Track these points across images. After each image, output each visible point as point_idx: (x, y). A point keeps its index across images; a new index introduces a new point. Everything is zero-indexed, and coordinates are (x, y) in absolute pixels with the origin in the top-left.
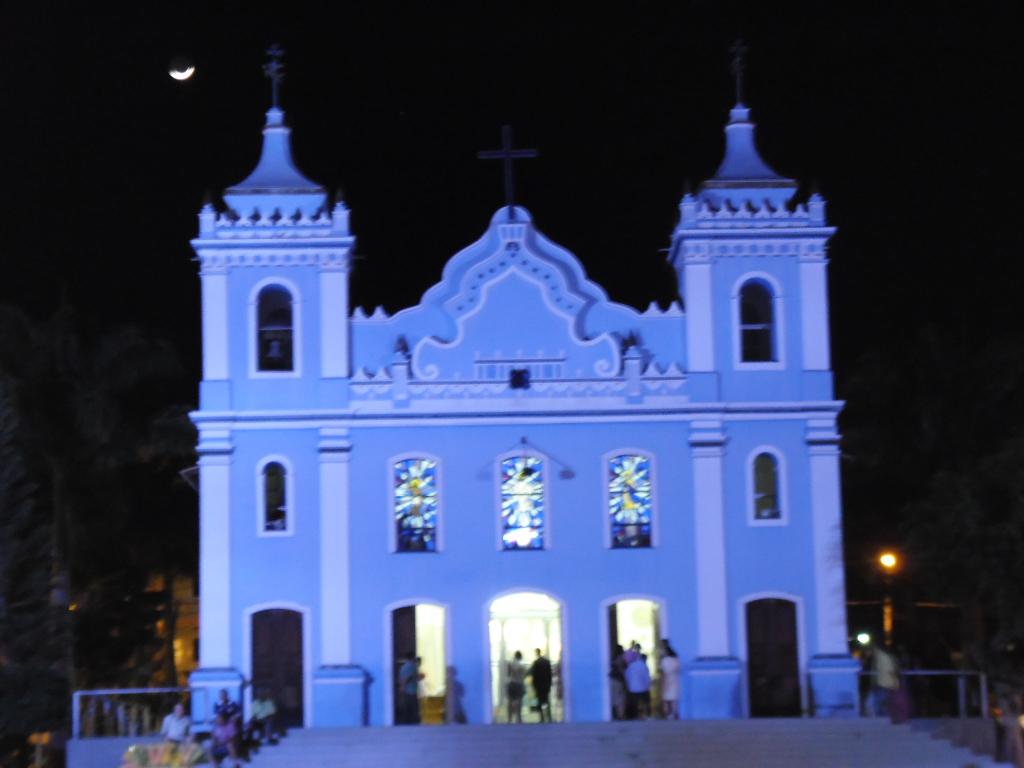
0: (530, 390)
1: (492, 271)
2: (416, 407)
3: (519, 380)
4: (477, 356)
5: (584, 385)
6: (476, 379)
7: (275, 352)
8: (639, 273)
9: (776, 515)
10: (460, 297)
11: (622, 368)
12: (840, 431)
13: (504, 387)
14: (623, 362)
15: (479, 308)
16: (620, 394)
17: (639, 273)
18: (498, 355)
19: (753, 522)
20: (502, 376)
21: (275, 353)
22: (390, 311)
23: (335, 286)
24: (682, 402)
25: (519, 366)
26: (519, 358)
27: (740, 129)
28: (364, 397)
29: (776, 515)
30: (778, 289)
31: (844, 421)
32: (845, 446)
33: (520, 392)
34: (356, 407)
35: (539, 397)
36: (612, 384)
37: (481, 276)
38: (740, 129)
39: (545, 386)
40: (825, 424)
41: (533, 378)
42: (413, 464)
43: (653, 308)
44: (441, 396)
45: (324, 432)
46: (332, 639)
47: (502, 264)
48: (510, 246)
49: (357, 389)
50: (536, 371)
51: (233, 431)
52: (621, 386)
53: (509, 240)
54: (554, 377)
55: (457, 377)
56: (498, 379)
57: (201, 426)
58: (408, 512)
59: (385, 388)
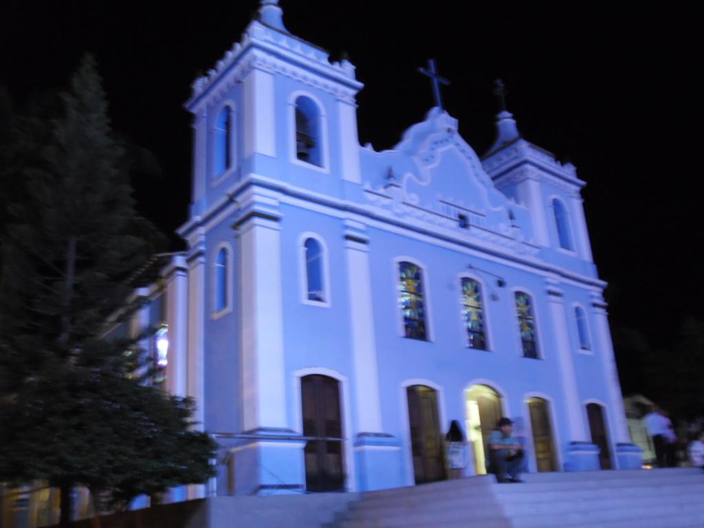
1: (442, 142)
2: (407, 221)
3: (463, 222)
4: (440, 196)
10: (424, 150)
12: (605, 301)
13: (454, 224)
16: (512, 248)
21: (307, 147)
22: (378, 148)
23: (347, 117)
25: (463, 213)
27: (507, 122)
28: (371, 203)
31: (606, 294)
32: (608, 309)
33: (464, 231)
35: (472, 236)
38: (507, 122)
40: (596, 293)
42: (409, 269)
45: (349, 223)
46: (369, 409)
50: (472, 218)
51: (280, 203)
55: (429, 207)
58: (409, 305)
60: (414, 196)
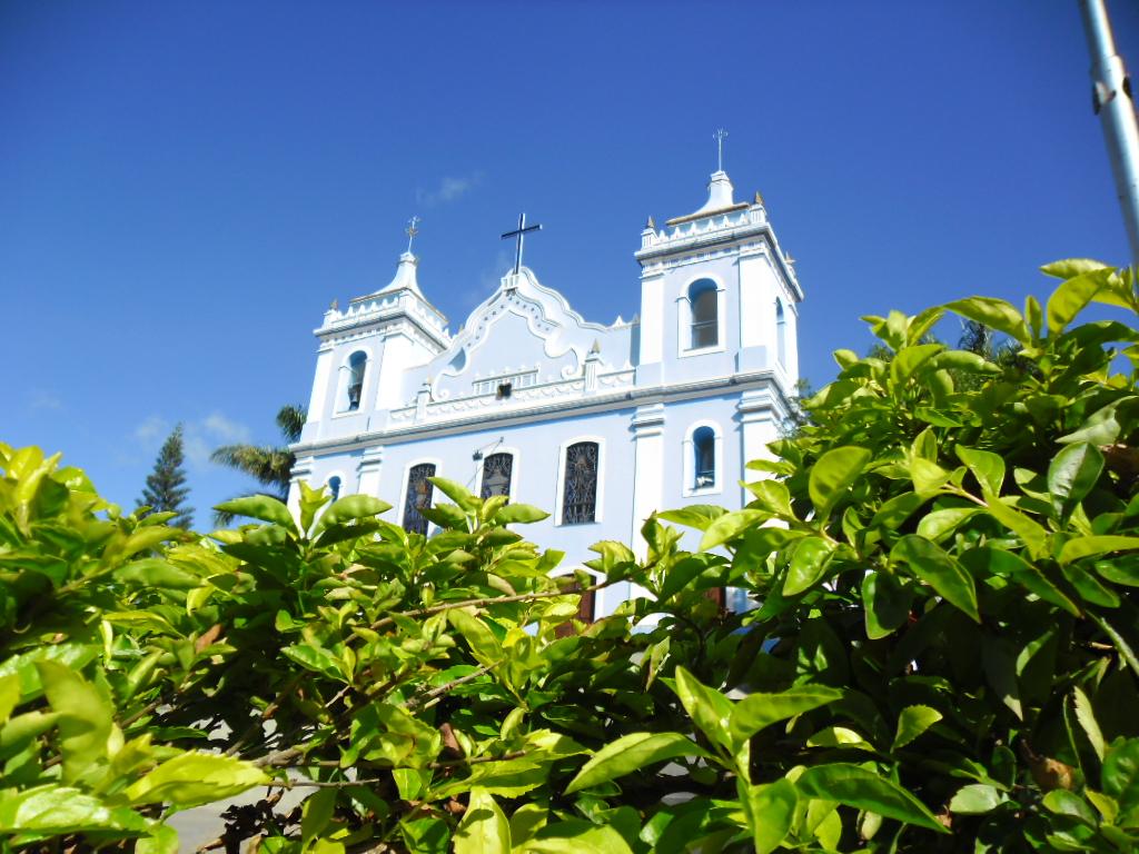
0: (512, 397)
3: (505, 391)
5: (553, 388)
6: (475, 394)
7: (355, 400)
8: (605, 293)
9: (712, 484)
11: (584, 374)
14: (584, 367)
15: (478, 345)
17: (605, 293)
18: (493, 375)
19: (687, 493)
20: (493, 389)
24: (630, 388)
25: (504, 383)
26: (503, 369)
29: (711, 484)
30: (720, 286)
33: (504, 400)
34: (389, 427)
36: (575, 385)
37: (486, 319)
39: (523, 393)
41: (514, 387)
43: (619, 321)
44: (449, 412)
47: (502, 307)
48: (509, 291)
49: (395, 415)
52: (582, 384)
53: (509, 287)
54: (532, 385)
56: (489, 393)
57: (297, 455)
59: (413, 411)
60: (442, 394)
